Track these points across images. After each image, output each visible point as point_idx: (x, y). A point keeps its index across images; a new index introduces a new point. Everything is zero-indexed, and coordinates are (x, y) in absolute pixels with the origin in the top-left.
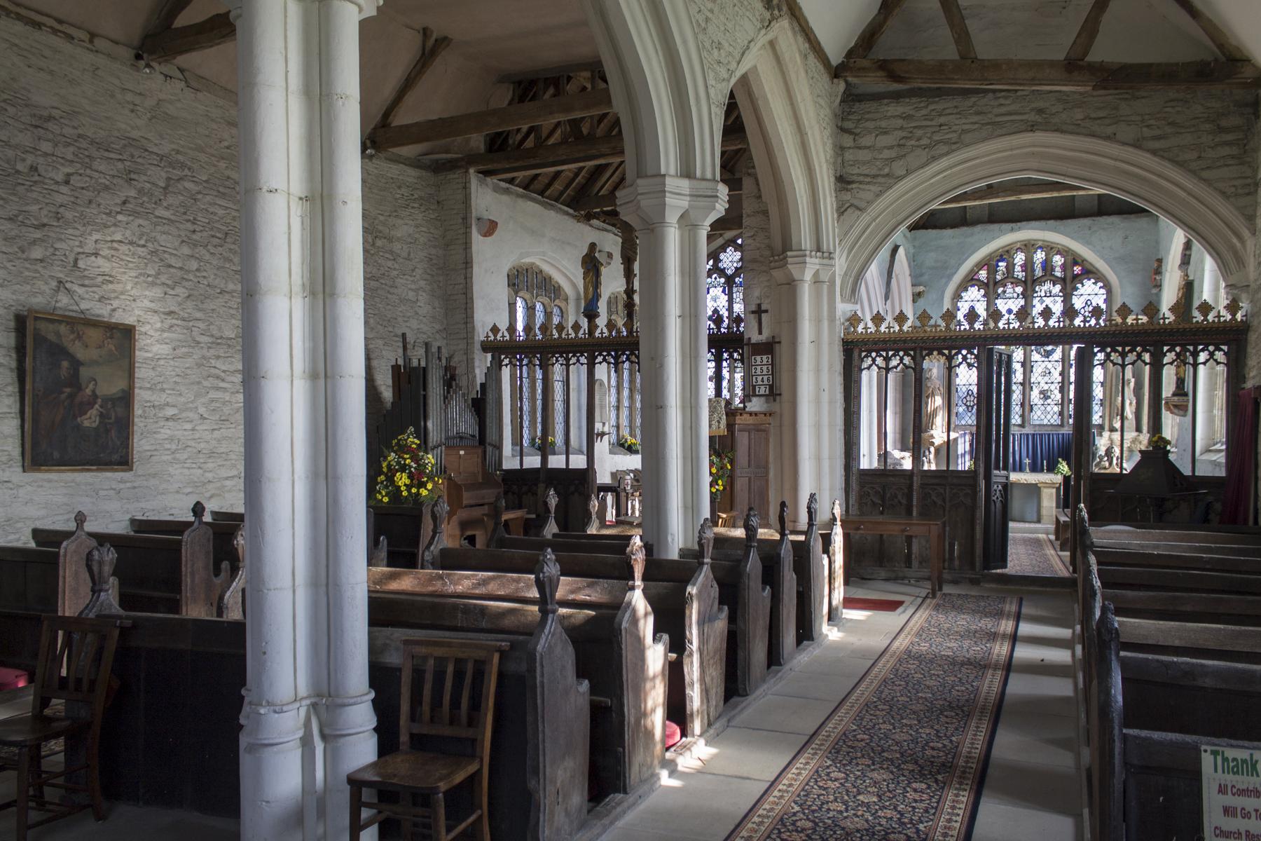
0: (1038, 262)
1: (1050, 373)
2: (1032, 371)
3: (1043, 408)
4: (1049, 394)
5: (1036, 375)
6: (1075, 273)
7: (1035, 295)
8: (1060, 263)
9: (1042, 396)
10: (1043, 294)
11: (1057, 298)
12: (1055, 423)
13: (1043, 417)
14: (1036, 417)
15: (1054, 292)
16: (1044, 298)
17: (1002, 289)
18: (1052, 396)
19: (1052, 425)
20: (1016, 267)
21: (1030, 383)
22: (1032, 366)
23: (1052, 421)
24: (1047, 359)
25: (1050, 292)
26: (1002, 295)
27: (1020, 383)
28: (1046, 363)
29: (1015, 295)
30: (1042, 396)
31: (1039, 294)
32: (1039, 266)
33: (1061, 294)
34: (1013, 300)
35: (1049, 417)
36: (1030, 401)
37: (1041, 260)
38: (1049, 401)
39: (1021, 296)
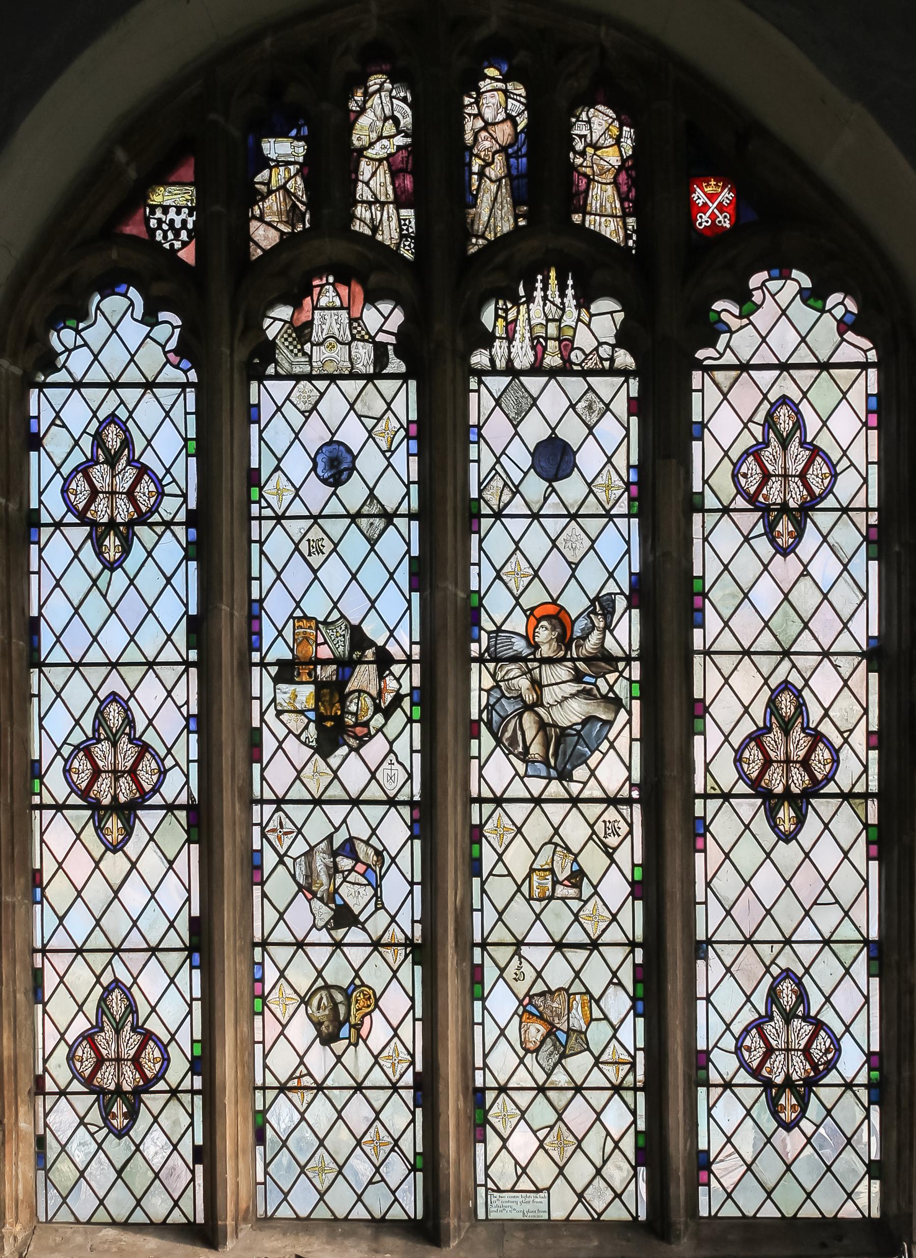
0: (486, 143)
1: (577, 877)
2: (475, 867)
3: (542, 1114)
4: (577, 1021)
5: (500, 889)
6: (703, 221)
7: (480, 359)
8: (612, 158)
9: (536, 1031)
10: (523, 358)
11: (604, 386)
12: (617, 1213)
13: (543, 1170)
14: (503, 1171)
15: (584, 340)
16: (533, 383)
17: (284, 312)
18: (598, 1034)
19: (597, 1224)
20: (366, 170)
21: (466, 945)
22: (476, 834)
23: (599, 1198)
24: (555, 789)
25: (566, 344)
26: (286, 358)
27: (409, 943)
28: (556, 811)
29: (364, 354)
30: (536, 1031)
31: (499, 348)
32: (496, 170)
33: (624, 359)
34: (352, 387)
35: (580, 1171)
36: (467, 1067)
37: (504, 133)
38: (579, 1064)
39: (396, 365)
